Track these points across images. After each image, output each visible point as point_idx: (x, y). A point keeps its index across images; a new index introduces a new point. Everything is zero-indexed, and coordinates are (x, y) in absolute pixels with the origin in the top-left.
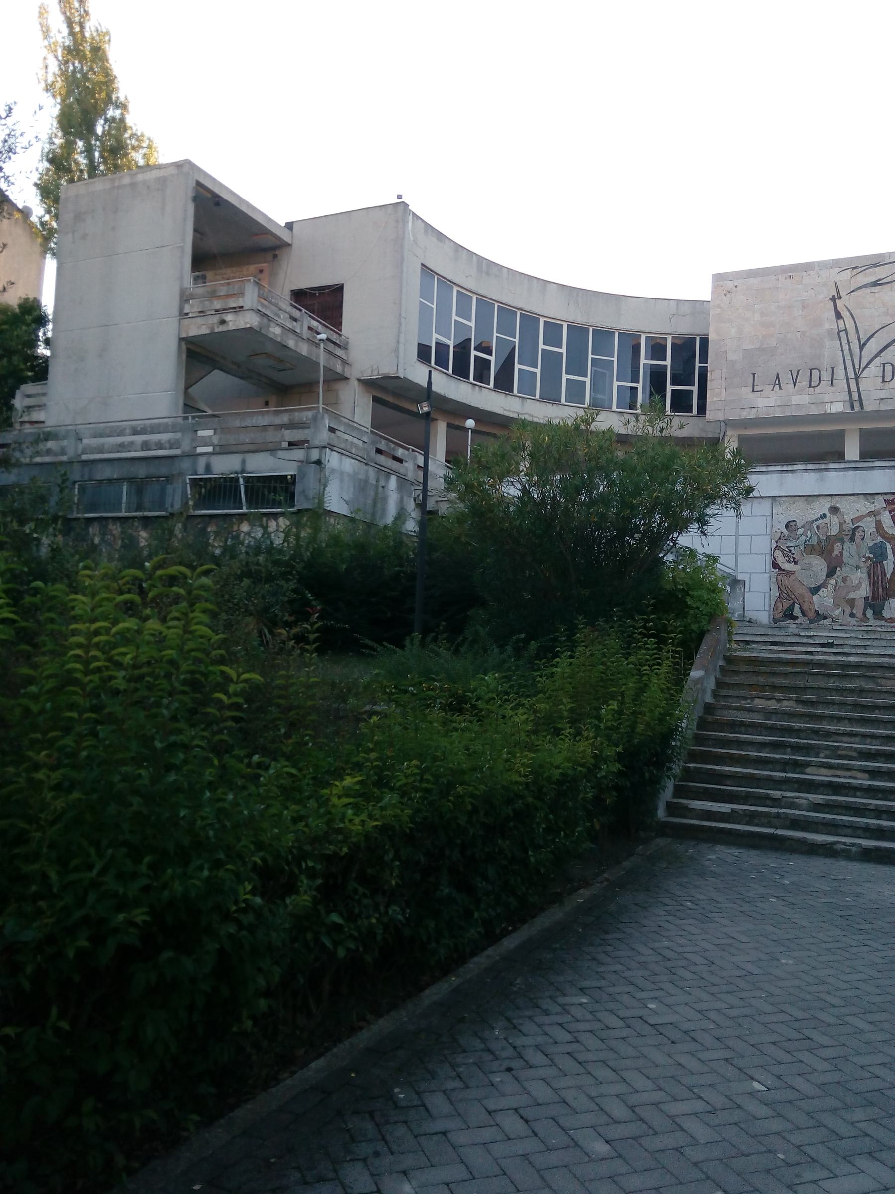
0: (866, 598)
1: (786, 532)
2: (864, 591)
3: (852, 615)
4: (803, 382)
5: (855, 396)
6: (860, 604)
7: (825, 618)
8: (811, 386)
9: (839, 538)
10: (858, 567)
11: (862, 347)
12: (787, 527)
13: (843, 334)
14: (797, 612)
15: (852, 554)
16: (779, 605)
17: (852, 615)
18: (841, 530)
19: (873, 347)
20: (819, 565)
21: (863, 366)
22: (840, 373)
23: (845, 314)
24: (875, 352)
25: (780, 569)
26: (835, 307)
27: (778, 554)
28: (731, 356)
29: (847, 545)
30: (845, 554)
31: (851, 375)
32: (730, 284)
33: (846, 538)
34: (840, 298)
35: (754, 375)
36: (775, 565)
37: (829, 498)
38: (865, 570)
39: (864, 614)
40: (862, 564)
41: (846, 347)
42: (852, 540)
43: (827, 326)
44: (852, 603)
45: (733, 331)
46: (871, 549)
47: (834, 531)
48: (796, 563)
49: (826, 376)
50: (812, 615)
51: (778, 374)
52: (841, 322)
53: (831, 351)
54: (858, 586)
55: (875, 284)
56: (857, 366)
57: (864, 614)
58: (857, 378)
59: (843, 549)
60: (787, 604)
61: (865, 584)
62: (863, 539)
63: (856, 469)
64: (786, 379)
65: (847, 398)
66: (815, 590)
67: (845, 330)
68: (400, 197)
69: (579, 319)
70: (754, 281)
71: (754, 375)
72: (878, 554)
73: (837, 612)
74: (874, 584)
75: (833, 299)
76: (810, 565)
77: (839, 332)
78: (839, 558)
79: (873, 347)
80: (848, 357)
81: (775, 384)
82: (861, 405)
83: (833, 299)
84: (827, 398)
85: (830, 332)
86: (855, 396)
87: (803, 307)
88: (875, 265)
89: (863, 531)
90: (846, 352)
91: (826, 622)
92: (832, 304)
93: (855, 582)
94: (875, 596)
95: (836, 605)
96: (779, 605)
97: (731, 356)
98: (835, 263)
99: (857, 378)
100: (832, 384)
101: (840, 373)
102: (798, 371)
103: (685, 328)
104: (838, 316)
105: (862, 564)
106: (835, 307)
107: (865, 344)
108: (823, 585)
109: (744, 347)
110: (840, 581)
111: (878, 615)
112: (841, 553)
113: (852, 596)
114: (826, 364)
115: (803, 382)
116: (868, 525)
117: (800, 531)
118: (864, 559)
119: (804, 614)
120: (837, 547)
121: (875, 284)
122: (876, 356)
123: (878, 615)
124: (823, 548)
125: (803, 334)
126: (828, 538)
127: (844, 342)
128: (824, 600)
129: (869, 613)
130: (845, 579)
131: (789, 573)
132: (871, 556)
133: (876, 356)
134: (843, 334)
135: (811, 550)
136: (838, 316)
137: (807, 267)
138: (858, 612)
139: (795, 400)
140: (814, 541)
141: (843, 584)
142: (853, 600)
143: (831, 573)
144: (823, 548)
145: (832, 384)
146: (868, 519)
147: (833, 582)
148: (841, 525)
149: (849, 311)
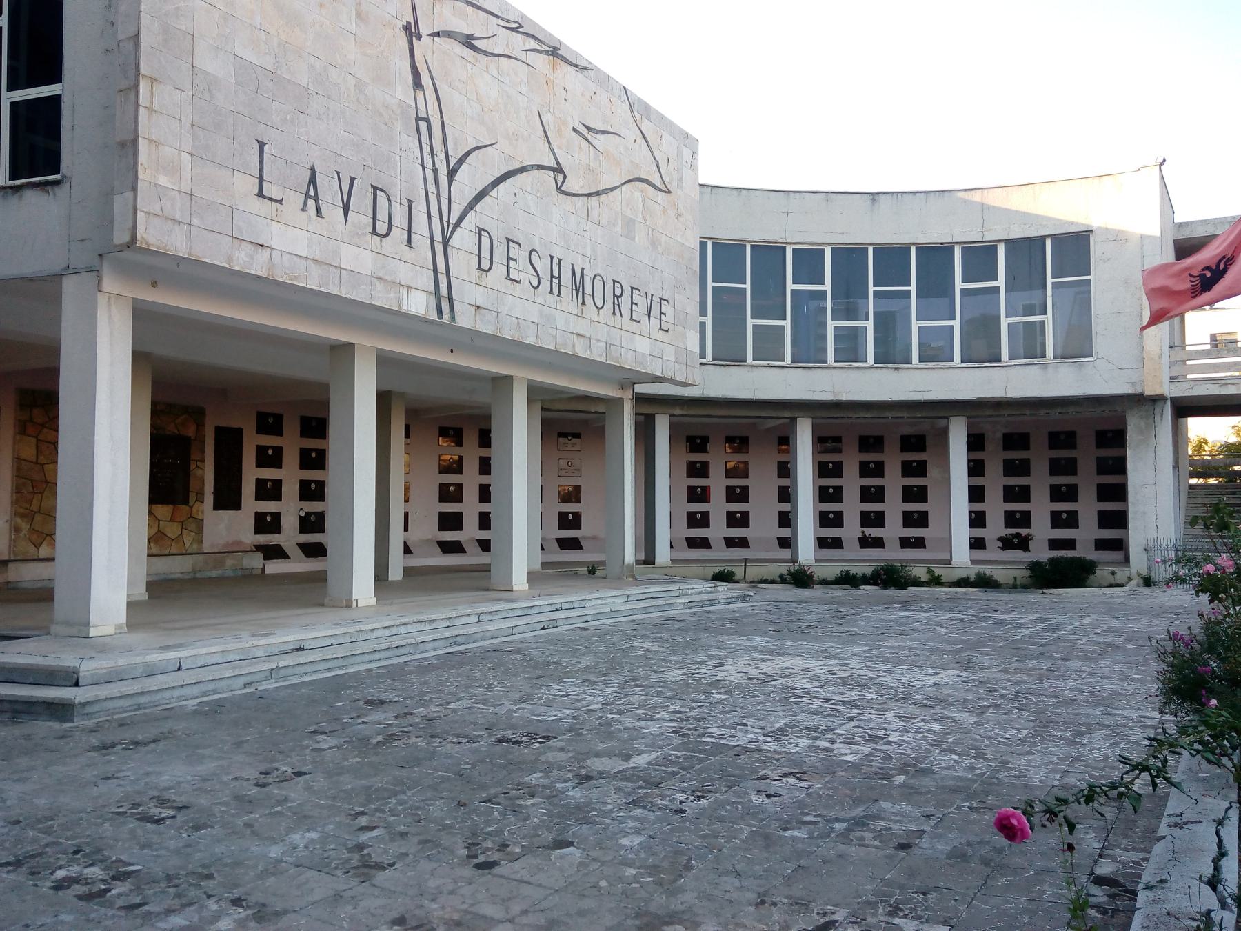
5: (444, 291)
8: (374, 232)
11: (452, 174)
13: (423, 125)
19: (468, 181)
21: (454, 220)
24: (470, 194)
31: (438, 237)
35: (262, 145)
51: (313, 170)
55: (468, 41)
56: (445, 218)
58: (445, 244)
65: (432, 288)
67: (427, 120)
71: (262, 145)
77: (418, 119)
79: (468, 181)
81: (307, 196)
82: (453, 318)
86: (444, 291)
97: (211, 64)
99: (445, 244)
102: (353, 179)
121: (468, 41)
134: (423, 125)
149: (433, 80)
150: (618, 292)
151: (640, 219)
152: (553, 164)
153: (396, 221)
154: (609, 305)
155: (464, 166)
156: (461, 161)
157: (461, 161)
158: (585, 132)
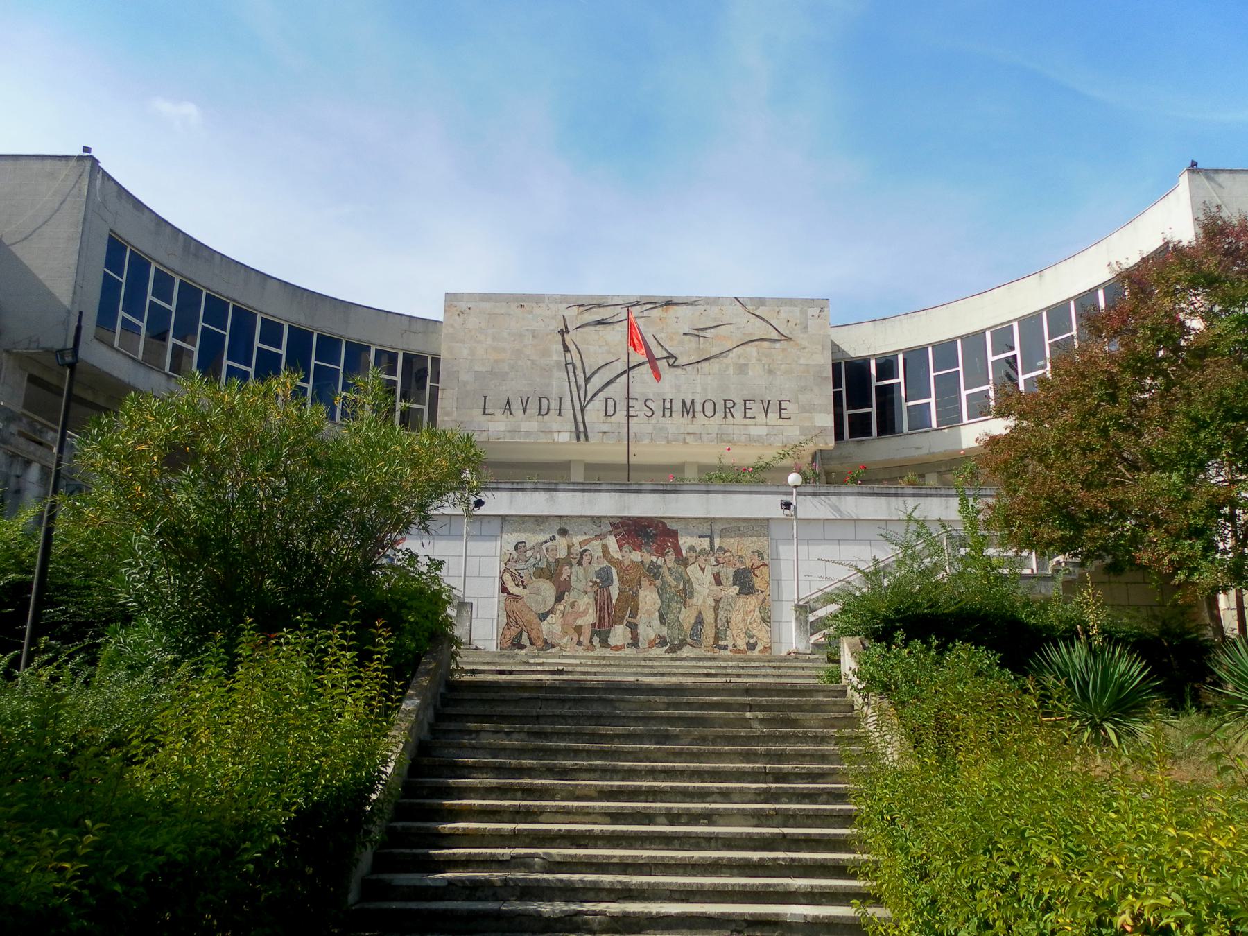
0: (593, 625)
1: (515, 554)
2: (591, 618)
3: (579, 643)
4: (533, 408)
5: (582, 429)
6: (587, 631)
7: (553, 646)
9: (567, 561)
10: (585, 593)
11: (587, 380)
12: (516, 548)
13: (570, 367)
14: (525, 640)
15: (579, 577)
16: (507, 632)
17: (579, 643)
18: (569, 553)
19: (597, 382)
20: (547, 589)
22: (567, 403)
23: (572, 347)
24: (598, 387)
25: (509, 593)
26: (564, 340)
27: (507, 577)
28: (464, 377)
29: (575, 568)
30: (573, 578)
31: (578, 407)
32: (463, 306)
33: (574, 562)
34: (568, 332)
36: (504, 589)
37: (558, 520)
38: (592, 595)
39: (591, 642)
40: (589, 589)
41: (572, 379)
42: (580, 563)
43: (555, 357)
44: (579, 630)
45: (465, 352)
46: (598, 574)
47: (562, 554)
48: (524, 587)
49: (554, 405)
50: (540, 643)
52: (568, 355)
53: (559, 383)
54: (585, 612)
55: (599, 323)
57: (591, 642)
58: (582, 410)
60: (514, 631)
61: (592, 610)
63: (584, 491)
64: (517, 407)
66: (543, 617)
68: (87, 149)
69: (303, 322)
70: (487, 306)
72: (604, 579)
73: (565, 640)
74: (600, 610)
75: (562, 333)
76: (538, 589)
79: (597, 382)
80: (574, 390)
83: (562, 333)
84: (555, 427)
85: (558, 363)
86: (582, 429)
87: (533, 336)
88: (600, 306)
90: (573, 384)
91: (553, 650)
92: (559, 337)
93: (582, 608)
94: (601, 624)
95: (565, 633)
96: (507, 632)
98: (564, 298)
99: (582, 410)
100: (560, 414)
101: (567, 403)
103: (417, 345)
104: (566, 349)
105: (589, 589)
106: (564, 340)
107: (590, 378)
108: (551, 611)
109: (477, 369)
111: (605, 643)
113: (579, 622)
114: (554, 394)
115: (533, 408)
116: (595, 548)
117: (529, 553)
119: (532, 643)
120: (566, 572)
121: (599, 323)
122: (600, 391)
123: (605, 643)
124: (552, 572)
125: (533, 362)
126: (557, 561)
127: (571, 374)
128: (552, 627)
129: (596, 640)
130: (572, 605)
131: (518, 598)
133: (600, 391)
134: (570, 367)
135: (540, 573)
136: (566, 349)
137: (538, 299)
138: (585, 639)
139: (525, 426)
140: (543, 565)
142: (581, 627)
143: (559, 598)
144: (552, 572)
145: (560, 414)
146: (595, 543)
147: (561, 607)
148: (569, 547)
150: (729, 404)
151: (753, 361)
152: (666, 355)
153: (552, 407)
154: (720, 414)
155: (597, 375)
156: (594, 374)
157: (594, 374)
158: (696, 332)
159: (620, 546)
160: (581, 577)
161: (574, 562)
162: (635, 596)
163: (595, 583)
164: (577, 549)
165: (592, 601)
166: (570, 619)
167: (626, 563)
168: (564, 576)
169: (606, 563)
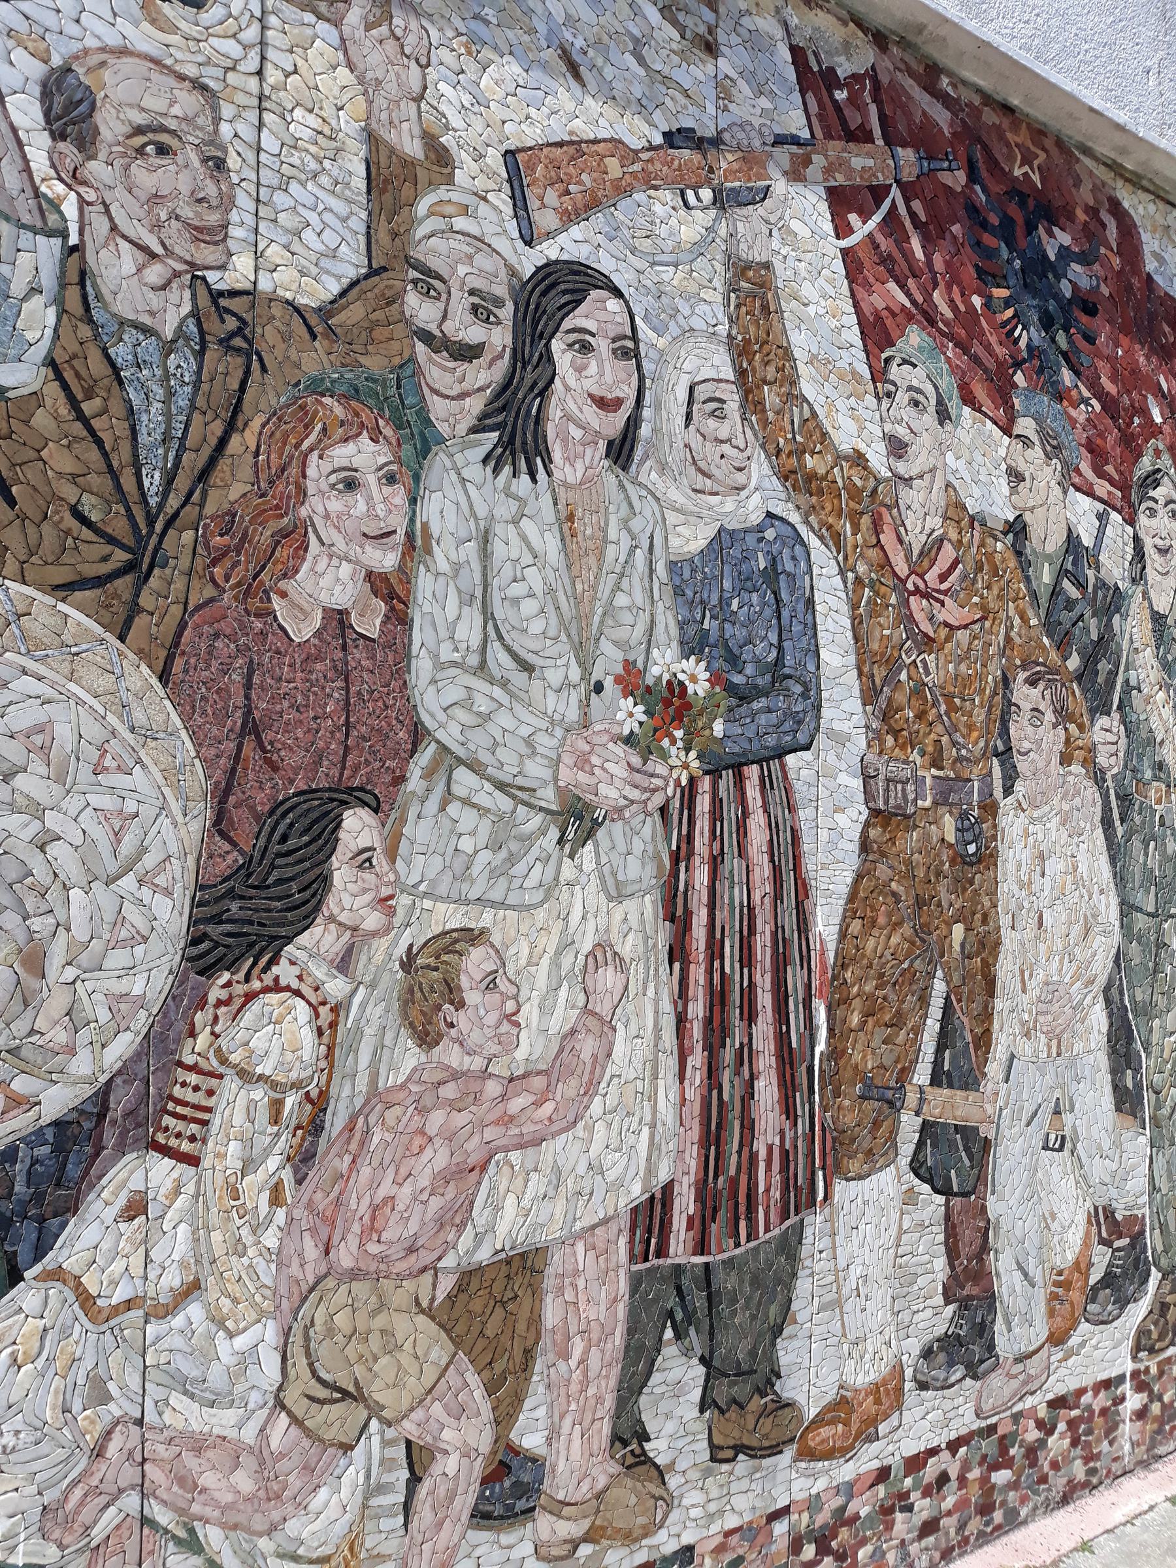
10: (578, 820)
29: (462, 490)
30: (441, 617)
40: (612, 780)
42: (516, 430)
59: (416, 545)
62: (621, 450)
78: (369, 656)
89: (628, 349)
95: (327, 1397)
105: (612, 780)
108: (142, 1108)
110: (373, 1012)
112: (392, 592)
118: (630, 714)
130: (430, 991)
132: (696, 677)
141: (409, 1058)
143: (250, 911)
147: (273, 1035)
159: (877, 334)
160: (532, 624)
161: (456, 396)
162: (976, 857)
163: (670, 705)
164: (476, 241)
165: (638, 924)
166: (396, 1186)
167: (920, 517)
168: (325, 584)
169: (760, 495)
